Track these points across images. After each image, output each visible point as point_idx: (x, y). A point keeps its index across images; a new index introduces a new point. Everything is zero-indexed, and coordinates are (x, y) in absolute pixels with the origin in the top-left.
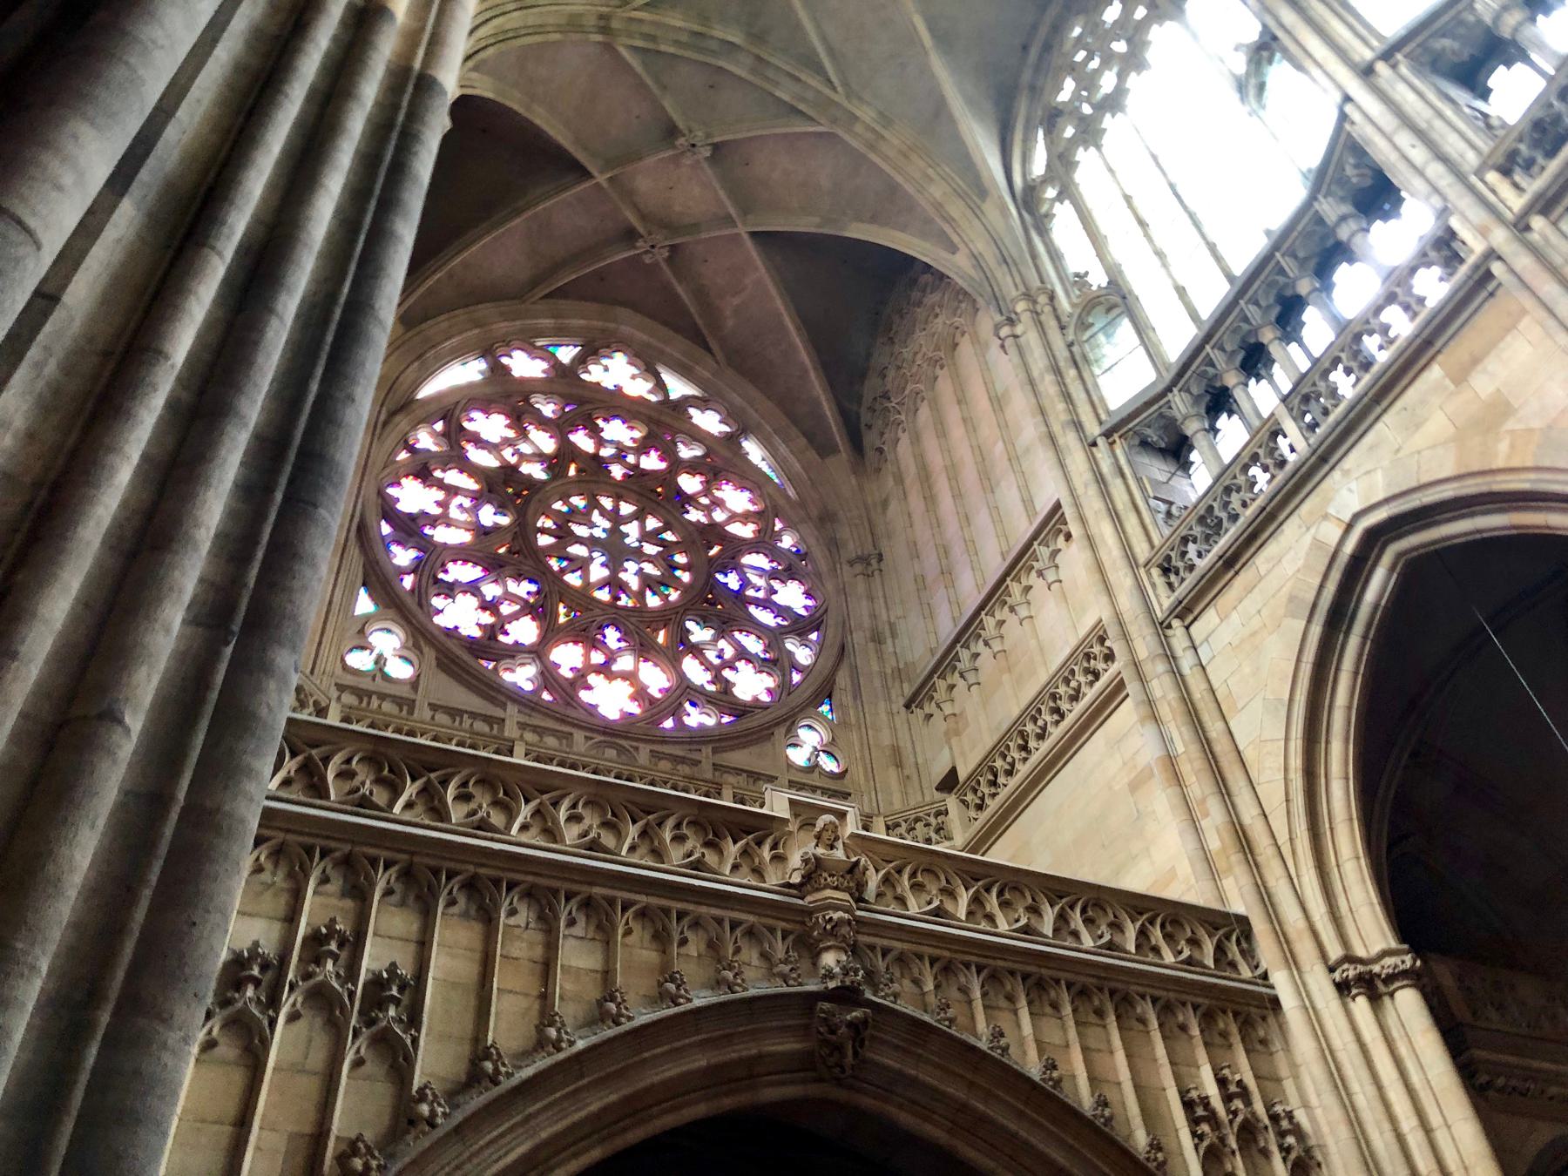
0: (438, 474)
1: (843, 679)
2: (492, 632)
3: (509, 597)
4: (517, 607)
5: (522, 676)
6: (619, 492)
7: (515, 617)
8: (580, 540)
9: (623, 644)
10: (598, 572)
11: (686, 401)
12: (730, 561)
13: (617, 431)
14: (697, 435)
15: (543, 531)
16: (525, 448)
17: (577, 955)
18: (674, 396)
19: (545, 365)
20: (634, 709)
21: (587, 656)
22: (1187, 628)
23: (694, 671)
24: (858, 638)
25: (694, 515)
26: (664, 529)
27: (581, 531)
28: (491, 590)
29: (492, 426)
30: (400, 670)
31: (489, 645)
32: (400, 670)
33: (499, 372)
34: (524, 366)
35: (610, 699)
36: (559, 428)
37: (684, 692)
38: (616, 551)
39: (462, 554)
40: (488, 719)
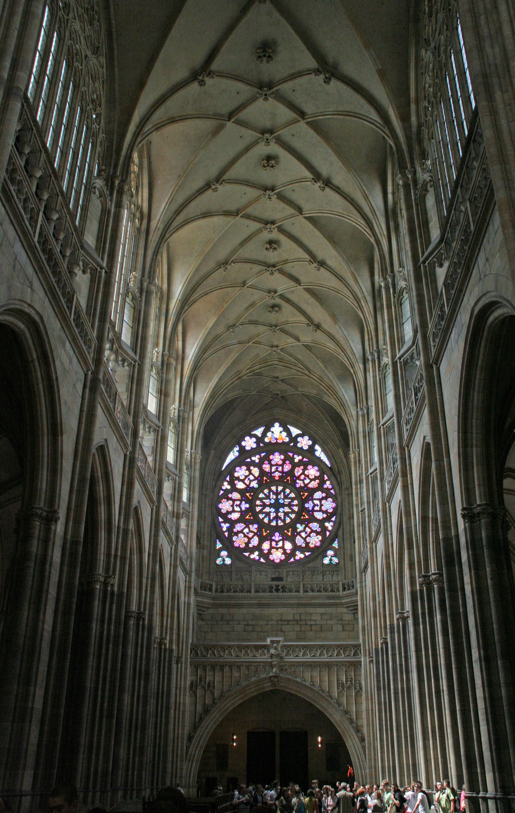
0: (230, 496)
1: (340, 533)
5: (255, 555)
6: (277, 483)
8: (268, 506)
9: (281, 538)
10: (273, 515)
11: (298, 436)
12: (310, 498)
13: (277, 458)
14: (300, 451)
15: (258, 506)
16: (251, 477)
17: (236, 674)
18: (294, 435)
19: (254, 440)
20: (283, 557)
21: (271, 544)
23: (299, 541)
24: (345, 518)
26: (290, 493)
27: (267, 502)
28: (246, 530)
29: (241, 472)
30: (228, 561)
32: (228, 561)
33: (242, 450)
34: (249, 443)
35: (277, 556)
36: (259, 465)
37: (296, 548)
38: (277, 506)
39: (238, 521)
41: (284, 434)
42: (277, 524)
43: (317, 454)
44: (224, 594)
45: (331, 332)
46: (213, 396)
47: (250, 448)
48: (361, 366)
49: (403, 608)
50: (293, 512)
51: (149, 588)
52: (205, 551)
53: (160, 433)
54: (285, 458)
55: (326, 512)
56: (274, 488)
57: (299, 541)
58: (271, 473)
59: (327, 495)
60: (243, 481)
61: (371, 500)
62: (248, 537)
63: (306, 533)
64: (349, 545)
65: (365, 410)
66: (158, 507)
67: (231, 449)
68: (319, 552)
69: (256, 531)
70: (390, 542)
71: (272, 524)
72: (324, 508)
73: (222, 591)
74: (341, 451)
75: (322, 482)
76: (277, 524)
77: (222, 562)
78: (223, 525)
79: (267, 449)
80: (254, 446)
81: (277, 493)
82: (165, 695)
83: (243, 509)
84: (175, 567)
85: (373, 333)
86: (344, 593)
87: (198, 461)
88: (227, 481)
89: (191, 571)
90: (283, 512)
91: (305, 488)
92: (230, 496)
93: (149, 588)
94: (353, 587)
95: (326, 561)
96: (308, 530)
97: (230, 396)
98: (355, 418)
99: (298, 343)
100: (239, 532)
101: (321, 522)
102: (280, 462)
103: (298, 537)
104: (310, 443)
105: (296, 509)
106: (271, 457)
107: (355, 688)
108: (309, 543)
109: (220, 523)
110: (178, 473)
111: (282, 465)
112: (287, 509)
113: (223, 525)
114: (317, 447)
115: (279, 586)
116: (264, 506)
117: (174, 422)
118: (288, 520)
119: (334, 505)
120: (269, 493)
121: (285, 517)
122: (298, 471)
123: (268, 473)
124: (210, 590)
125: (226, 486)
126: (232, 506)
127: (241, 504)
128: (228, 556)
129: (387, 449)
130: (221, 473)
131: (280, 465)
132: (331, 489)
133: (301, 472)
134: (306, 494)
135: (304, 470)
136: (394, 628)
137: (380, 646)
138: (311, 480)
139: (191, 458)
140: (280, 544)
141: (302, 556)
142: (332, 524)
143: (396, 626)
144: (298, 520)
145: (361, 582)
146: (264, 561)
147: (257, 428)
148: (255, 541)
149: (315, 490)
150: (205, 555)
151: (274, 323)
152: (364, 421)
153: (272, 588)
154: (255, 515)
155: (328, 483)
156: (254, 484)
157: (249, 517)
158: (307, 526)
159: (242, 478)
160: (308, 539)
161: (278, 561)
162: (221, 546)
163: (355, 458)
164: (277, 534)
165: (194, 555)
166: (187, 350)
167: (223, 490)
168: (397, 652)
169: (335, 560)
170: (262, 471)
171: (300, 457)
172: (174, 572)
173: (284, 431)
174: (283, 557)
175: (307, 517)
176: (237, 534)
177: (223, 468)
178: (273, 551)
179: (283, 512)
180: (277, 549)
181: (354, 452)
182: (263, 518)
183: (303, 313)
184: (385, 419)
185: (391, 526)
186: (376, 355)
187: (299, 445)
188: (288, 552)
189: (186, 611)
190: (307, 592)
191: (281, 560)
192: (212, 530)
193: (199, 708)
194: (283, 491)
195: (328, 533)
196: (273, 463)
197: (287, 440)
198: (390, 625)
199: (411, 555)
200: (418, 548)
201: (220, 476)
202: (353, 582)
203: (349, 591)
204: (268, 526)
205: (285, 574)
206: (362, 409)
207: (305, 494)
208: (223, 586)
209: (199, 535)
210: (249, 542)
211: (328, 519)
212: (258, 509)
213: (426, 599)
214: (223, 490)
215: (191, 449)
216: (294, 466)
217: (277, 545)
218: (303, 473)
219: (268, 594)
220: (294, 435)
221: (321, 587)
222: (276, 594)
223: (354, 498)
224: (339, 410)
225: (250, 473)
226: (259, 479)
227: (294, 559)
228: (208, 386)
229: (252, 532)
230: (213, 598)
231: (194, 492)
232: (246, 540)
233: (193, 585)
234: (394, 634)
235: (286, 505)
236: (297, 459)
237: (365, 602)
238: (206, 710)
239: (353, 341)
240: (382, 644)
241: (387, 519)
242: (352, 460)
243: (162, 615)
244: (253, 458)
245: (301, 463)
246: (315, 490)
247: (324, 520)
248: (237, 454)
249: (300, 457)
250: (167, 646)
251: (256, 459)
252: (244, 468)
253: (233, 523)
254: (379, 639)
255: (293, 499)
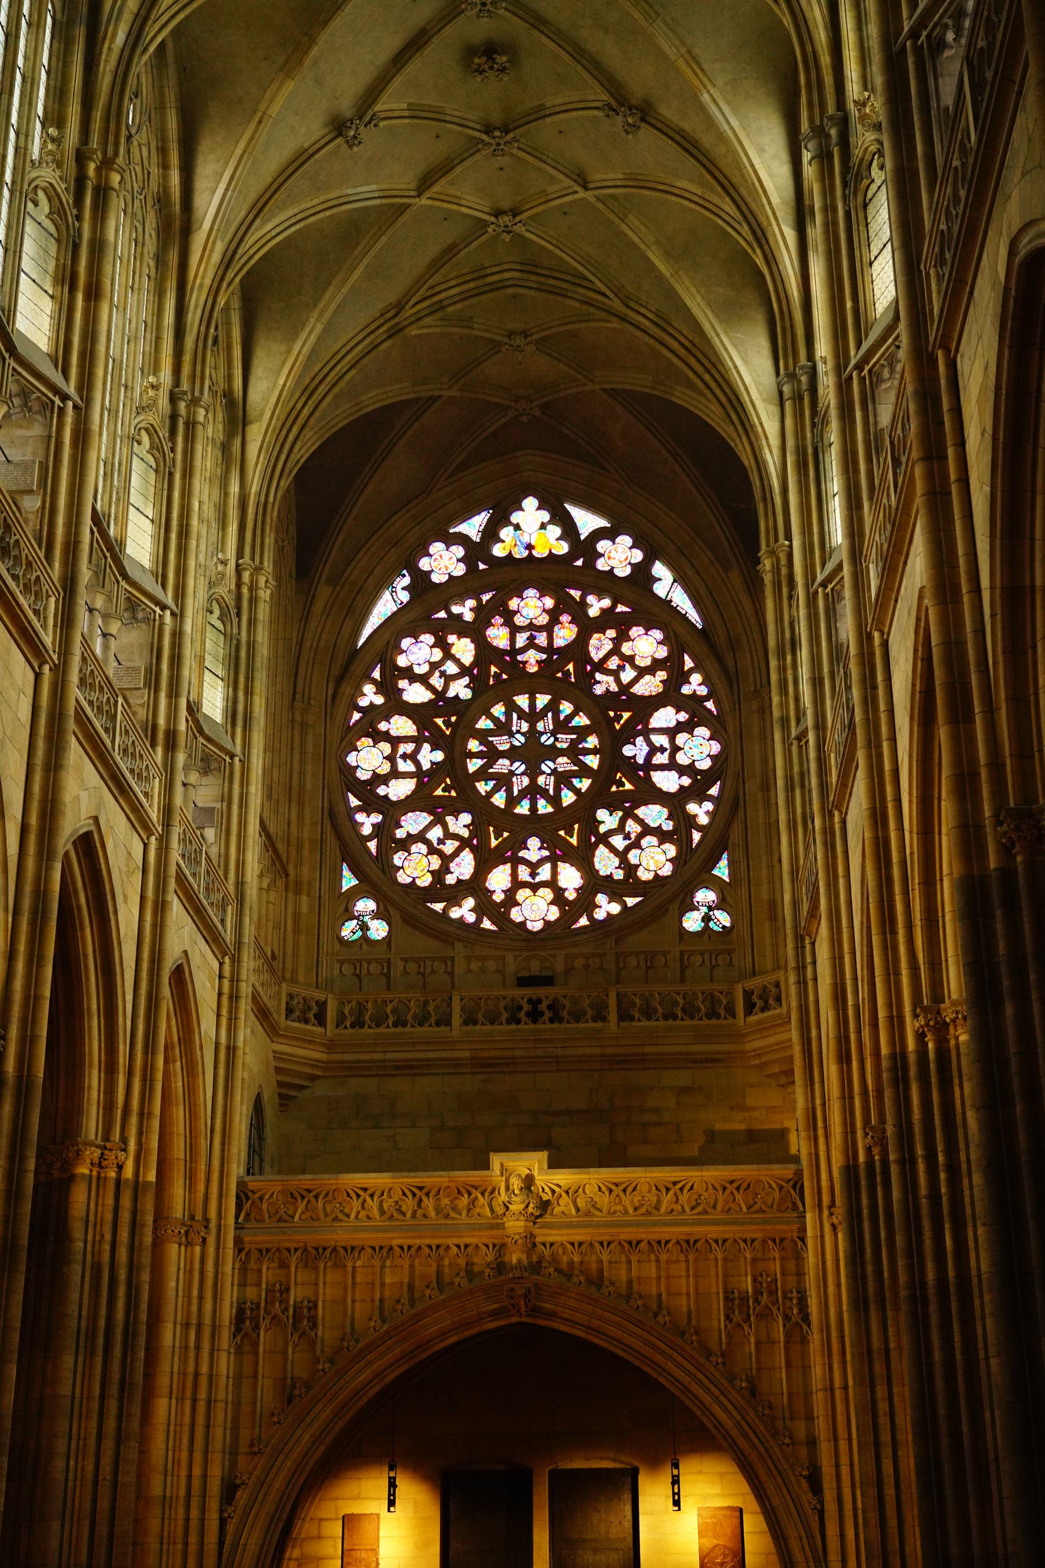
0: (383, 726)
1: (736, 833)
2: (437, 876)
3: (448, 835)
4: (457, 844)
5: (465, 911)
6: (532, 685)
7: (457, 853)
8: (503, 755)
11: (598, 535)
12: (639, 727)
13: (532, 606)
16: (451, 668)
18: (584, 533)
19: (459, 551)
20: (554, 914)
21: (514, 874)
22: (813, 944)
23: (605, 863)
24: (752, 786)
25: (604, 684)
27: (502, 743)
29: (418, 652)
30: (379, 930)
31: (440, 889)
33: (421, 583)
34: (443, 562)
35: (535, 910)
36: (475, 631)
38: (533, 754)
39: (409, 804)
40: (444, 960)
41: (555, 531)
42: (533, 808)
43: (660, 589)
44: (366, 1030)
45: (686, 126)
46: (309, 387)
47: (444, 579)
48: (790, 234)
49: (938, 996)
50: (584, 771)
51: (22, 947)
52: (304, 898)
53: (69, 420)
54: (556, 605)
55: (689, 770)
56: (522, 701)
57: (605, 863)
58: (514, 651)
59: (692, 717)
60: (424, 680)
61: (826, 669)
62: (440, 854)
63: (627, 837)
64: (764, 872)
65: (804, 379)
66: (61, 671)
67: (385, 582)
68: (671, 894)
69: (465, 833)
70: (887, 766)
71: (518, 810)
72: (682, 759)
73: (358, 1023)
74: (735, 578)
75: (678, 678)
76: (533, 808)
77: (359, 934)
78: (360, 817)
79: (497, 578)
80: (460, 570)
81: (533, 716)
82: (118, 1339)
83: (426, 766)
84: (161, 907)
85: (825, 60)
86: (752, 1018)
87: (265, 594)
88: (374, 681)
89: (239, 944)
90: (554, 772)
91: (623, 697)
92: (383, 726)
93: (22, 947)
94: (778, 999)
95: (692, 922)
96: (632, 827)
97: (372, 400)
98: (774, 441)
99: (582, 194)
100: (412, 839)
101: (675, 802)
102: (544, 619)
103: (602, 851)
104: (638, 556)
105: (592, 761)
106: (514, 604)
107: (787, 1317)
108: (637, 866)
109: (352, 811)
110: (169, 600)
111: (549, 629)
112: (563, 763)
113: (360, 817)
114: (659, 569)
115: (539, 1001)
116: (492, 755)
117: (151, 431)
118: (568, 798)
119: (715, 747)
120: (508, 714)
121: (558, 790)
122: (599, 645)
123: (504, 652)
124: (320, 1019)
125: (370, 696)
126: (391, 758)
127: (417, 751)
128: (376, 915)
129: (873, 444)
130: (355, 653)
131: (540, 629)
132: (706, 698)
133: (608, 646)
134: (626, 715)
135: (617, 642)
136: (905, 1068)
137: (862, 1158)
138: (642, 672)
139: (239, 585)
140: (545, 873)
141: (615, 908)
142: (708, 806)
143: (912, 1058)
144: (601, 795)
145: (801, 968)
146: (493, 928)
147: (466, 515)
148: (464, 867)
149: (654, 703)
150: (304, 908)
151: (496, 118)
152: (799, 414)
153: (520, 1008)
154: (465, 783)
155: (696, 678)
156: (460, 689)
157: (446, 790)
158: (629, 814)
159: (421, 670)
160: (633, 857)
161: (536, 926)
162: (354, 882)
163: (776, 569)
164: (534, 843)
165: (252, 892)
166: (199, 200)
167: (360, 709)
168: (920, 1151)
169: (723, 918)
170: (484, 648)
171: (606, 603)
172: (154, 926)
173: (550, 522)
174: (554, 914)
175: (628, 786)
176: (405, 845)
177: (360, 644)
178: (522, 894)
179: (554, 772)
180: (534, 888)
181: (772, 553)
182: (490, 794)
183: (596, 68)
184: (865, 346)
185: (891, 711)
186: (833, 132)
187: (601, 565)
188: (571, 895)
189: (221, 1072)
190: (632, 1018)
191: (547, 923)
192: (322, 829)
193: (267, 1394)
194: (553, 707)
195: (696, 836)
196: (519, 620)
197: (562, 548)
198: (893, 1056)
199: (963, 744)
200: (990, 711)
201: (349, 668)
202: (777, 985)
203: (767, 1014)
204: (505, 818)
205: (560, 967)
206: (792, 376)
207: (621, 716)
208: (361, 1008)
209: (281, 847)
210: (445, 869)
211: (696, 792)
212: (474, 765)
213: (1024, 901)
214: (360, 709)
215: (240, 554)
216: (587, 627)
217: (533, 875)
218: (615, 651)
219: (506, 1027)
220: (584, 533)
221: (676, 1003)
222: (532, 1026)
223: (776, 699)
224: (725, 429)
225: (448, 655)
226: (476, 673)
227: (591, 918)
228: (289, 351)
229: (456, 837)
230: (330, 1046)
231: (249, 692)
232: (436, 862)
233: (245, 989)
234: (907, 1088)
235: (562, 753)
236: (596, 606)
237: (814, 1032)
238: (288, 1393)
239: (761, 151)
240: (869, 1150)
241: (874, 687)
242: (768, 578)
243: (110, 1068)
244: (456, 609)
245: (606, 621)
246: (654, 703)
247: (684, 795)
248: (405, 597)
249: (606, 603)
250: (129, 1172)
251: (465, 610)
252: (428, 639)
253: (393, 811)
254: (860, 1134)
255: (583, 733)
